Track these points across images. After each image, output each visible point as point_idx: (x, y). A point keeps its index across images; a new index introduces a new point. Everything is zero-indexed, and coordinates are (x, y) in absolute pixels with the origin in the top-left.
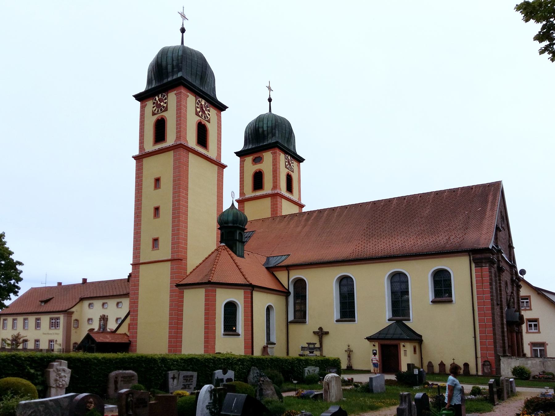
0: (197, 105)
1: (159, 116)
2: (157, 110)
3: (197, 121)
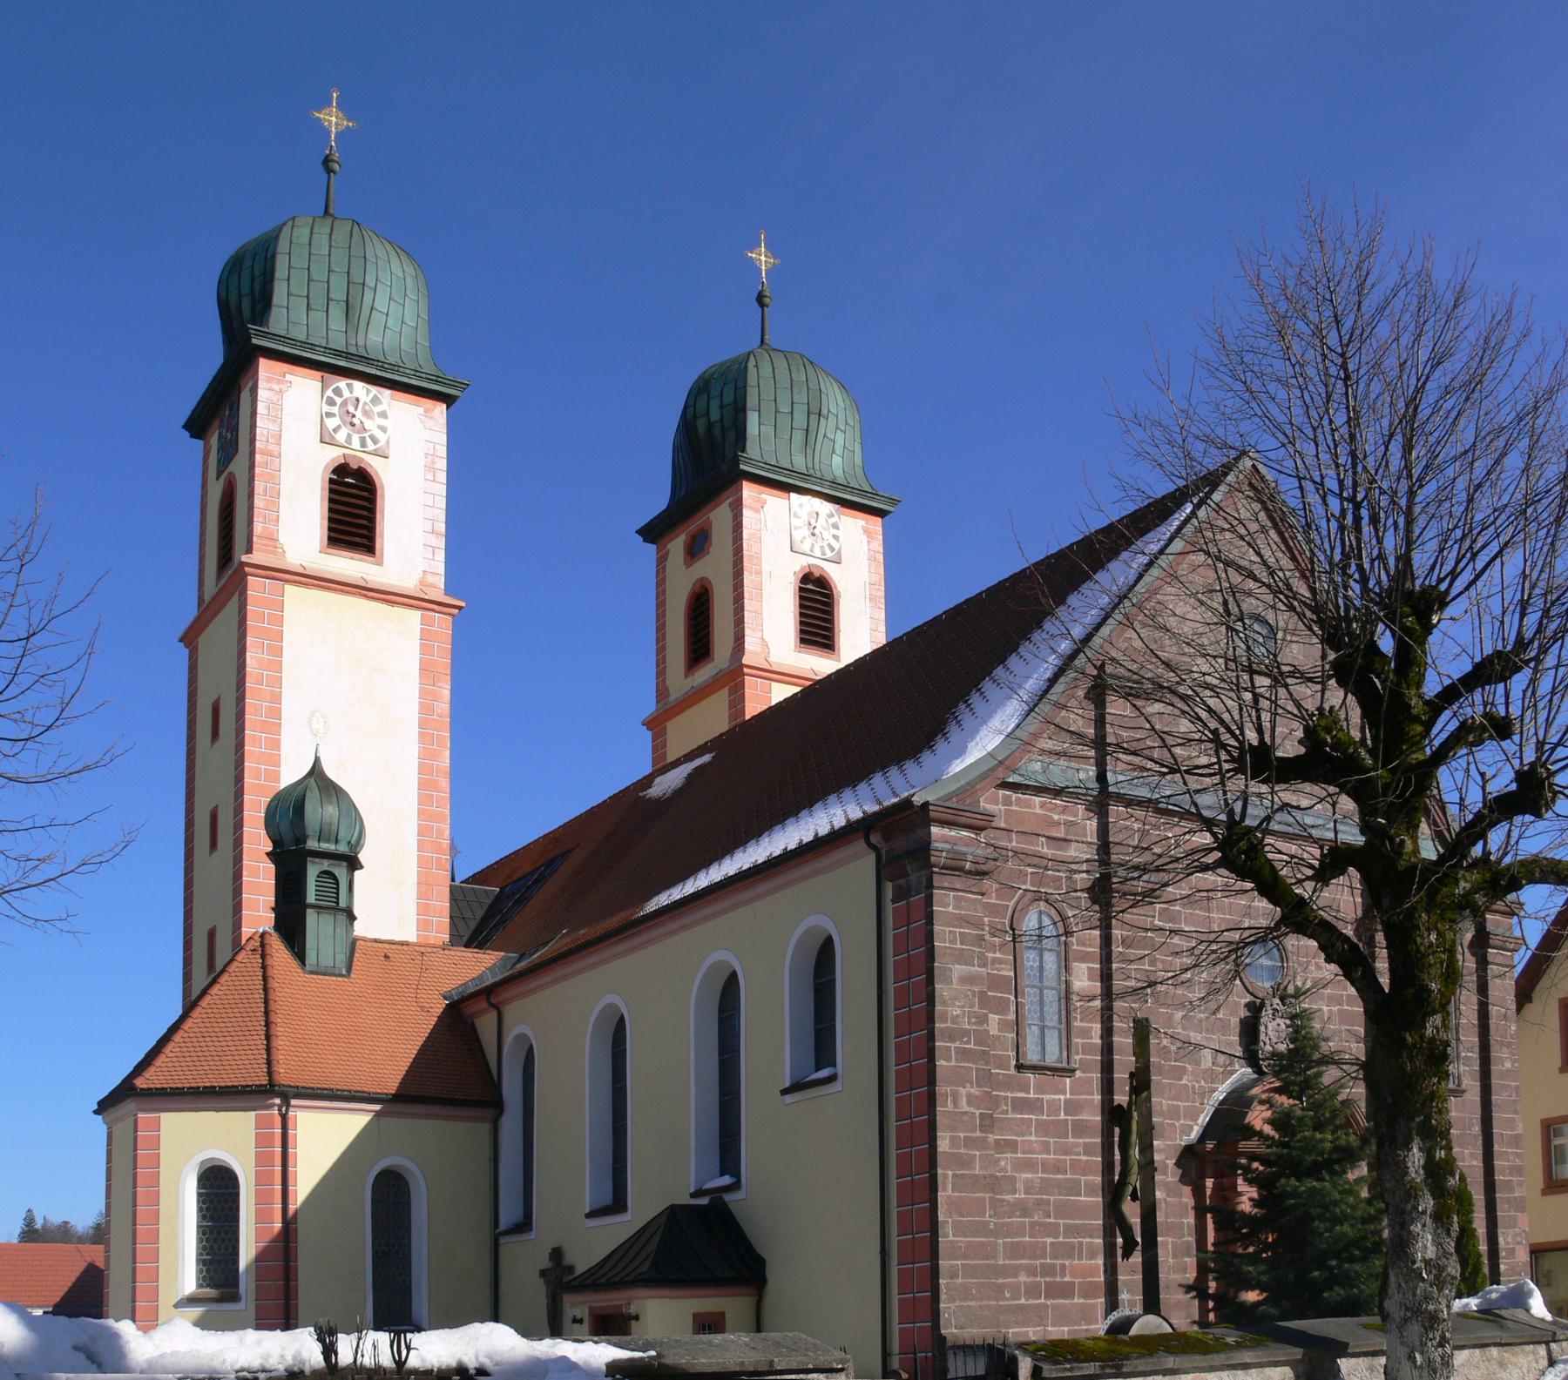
0: (326, 408)
3: (327, 467)
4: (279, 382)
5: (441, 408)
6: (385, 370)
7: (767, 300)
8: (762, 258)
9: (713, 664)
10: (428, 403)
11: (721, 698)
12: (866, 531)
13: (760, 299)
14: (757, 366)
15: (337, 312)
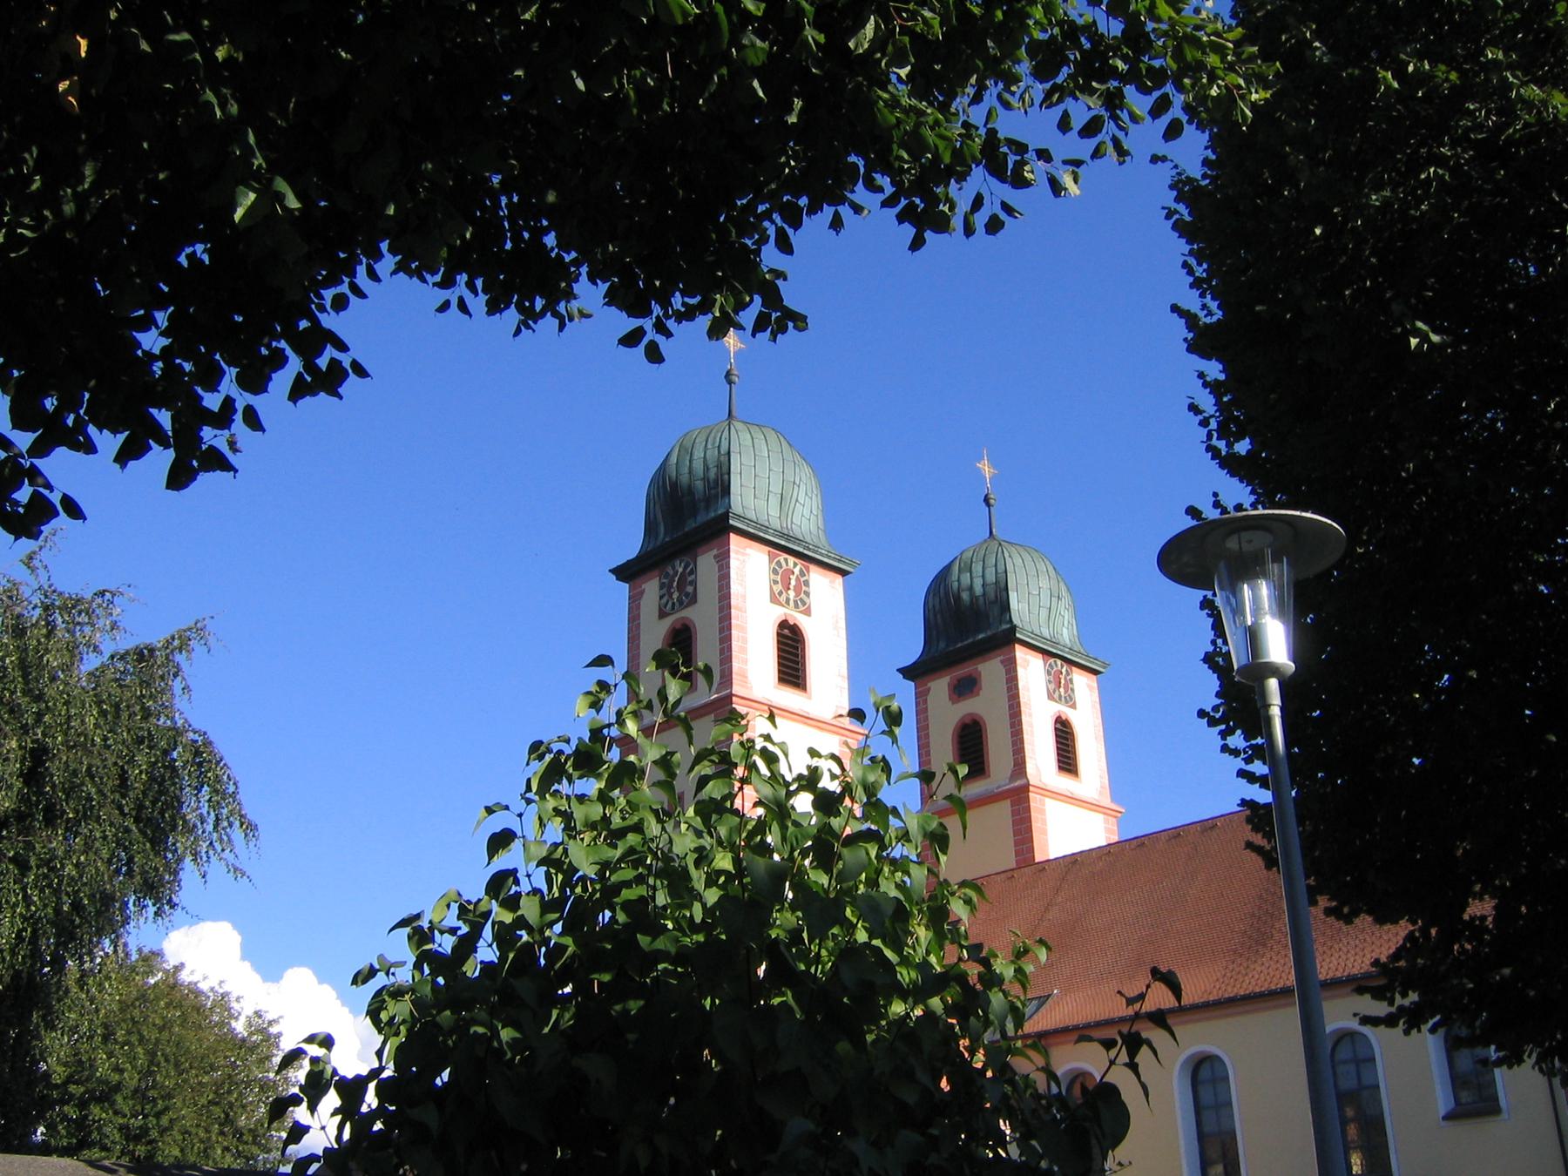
1: (677, 620)
2: (670, 603)
4: (744, 554)
5: (839, 580)
6: (809, 549)
7: (992, 501)
8: (986, 469)
9: (988, 781)
10: (832, 575)
11: (1004, 809)
12: (1090, 687)
13: (987, 500)
14: (1010, 556)
15: (774, 501)
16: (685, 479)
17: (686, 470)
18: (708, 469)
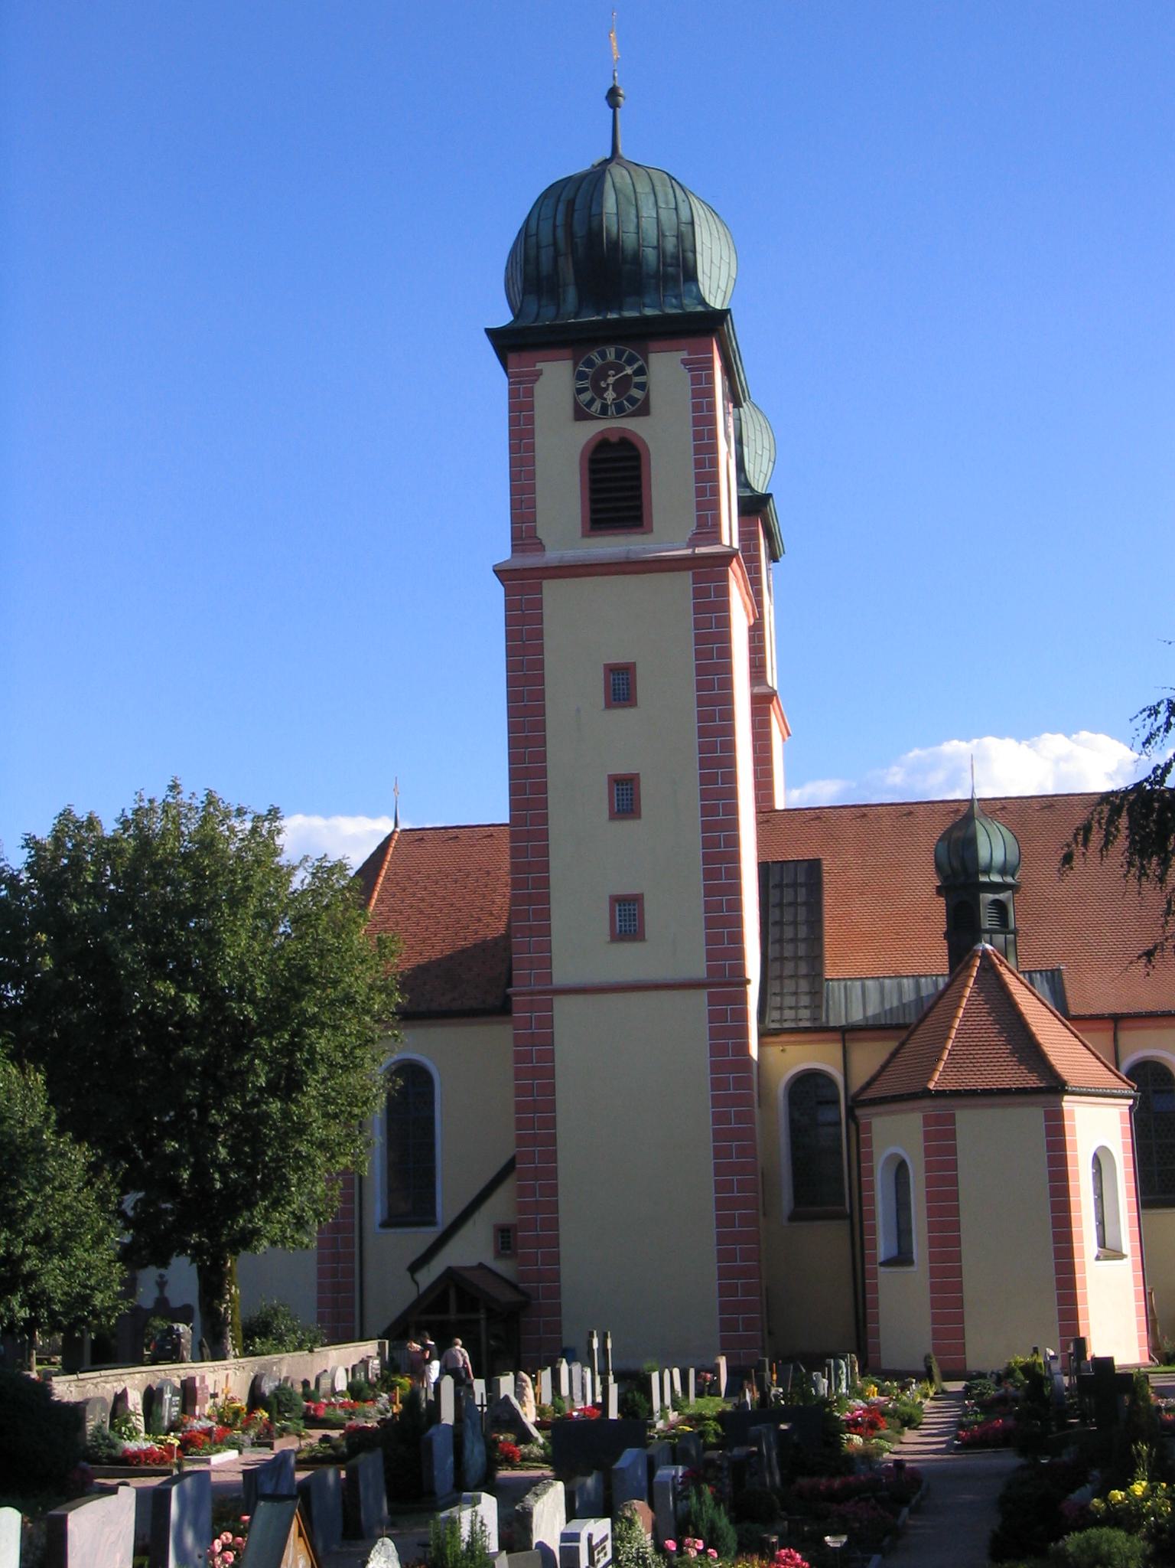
16: (629, 240)
17: (632, 228)
18: (664, 236)
